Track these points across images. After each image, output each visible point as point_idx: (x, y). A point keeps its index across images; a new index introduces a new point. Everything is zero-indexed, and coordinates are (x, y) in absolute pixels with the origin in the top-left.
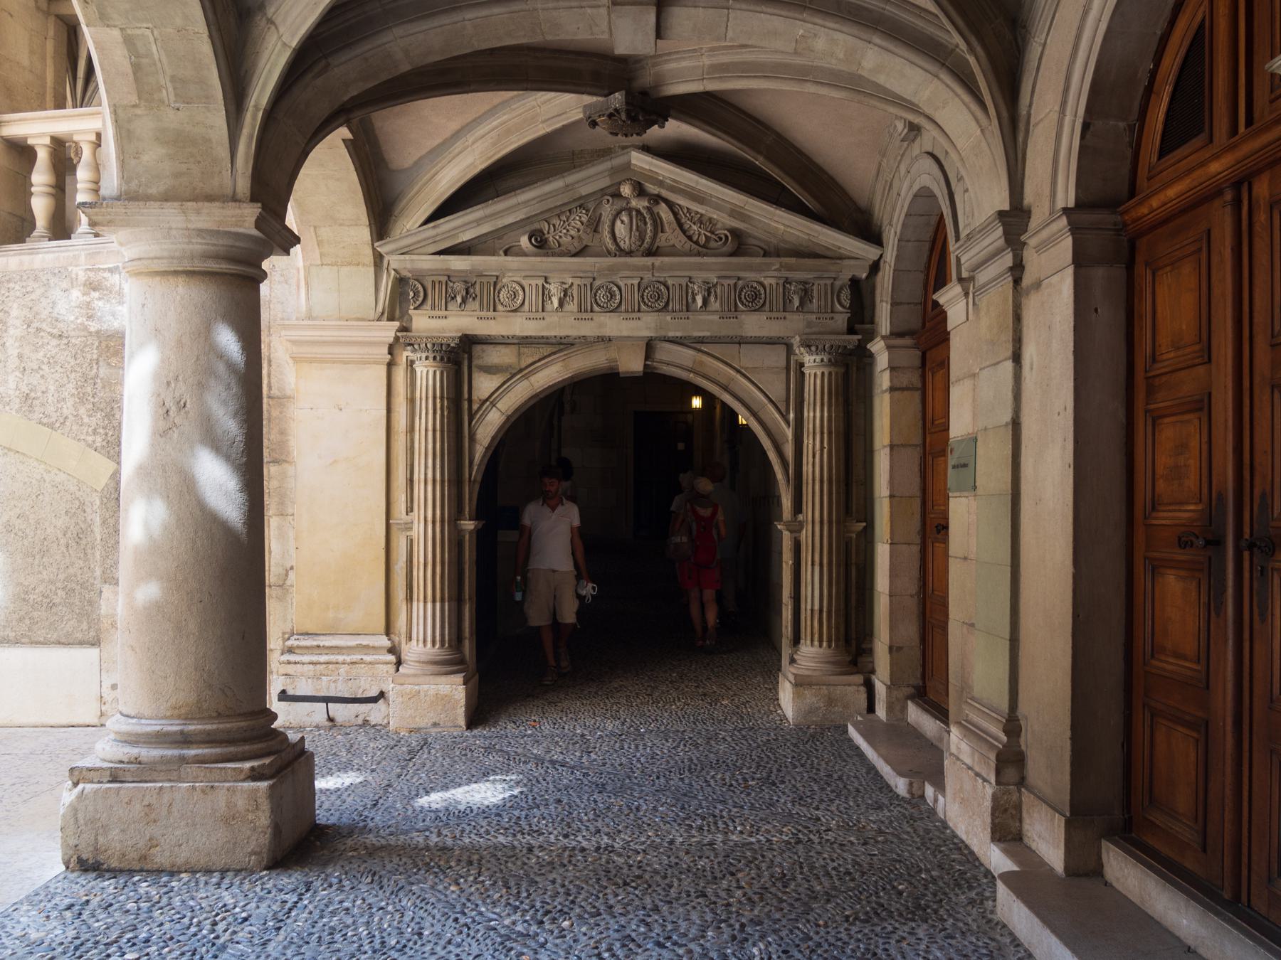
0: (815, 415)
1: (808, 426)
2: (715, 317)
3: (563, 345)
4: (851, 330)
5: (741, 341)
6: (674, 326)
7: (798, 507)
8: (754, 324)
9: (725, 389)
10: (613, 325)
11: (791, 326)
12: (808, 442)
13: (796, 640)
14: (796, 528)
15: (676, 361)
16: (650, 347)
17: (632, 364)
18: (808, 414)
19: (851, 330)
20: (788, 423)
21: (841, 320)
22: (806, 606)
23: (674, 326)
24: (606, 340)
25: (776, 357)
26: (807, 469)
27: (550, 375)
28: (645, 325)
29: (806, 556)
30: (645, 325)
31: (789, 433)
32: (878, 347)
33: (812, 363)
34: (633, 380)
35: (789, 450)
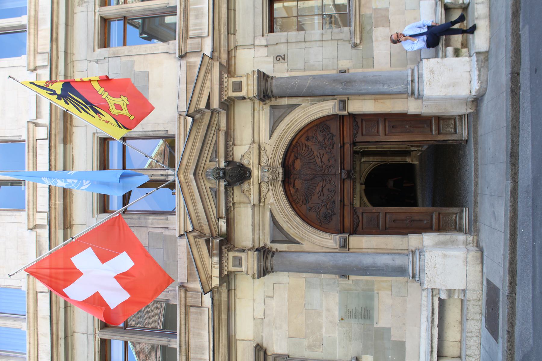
0: (371, 159)
1: (373, 160)
2: (357, 174)
3: (361, 197)
4: (358, 154)
5: (360, 170)
6: (358, 181)
7: (385, 161)
8: (358, 169)
9: (367, 172)
10: (358, 189)
11: (358, 163)
12: (375, 160)
13: (406, 161)
14: (389, 162)
15: (363, 180)
16: (361, 184)
17: (363, 187)
18: (371, 160)
19: (359, 154)
20: (372, 163)
21: (357, 155)
22: (401, 160)
23: (358, 181)
24: (360, 191)
25: (362, 165)
26: (380, 160)
27: (365, 199)
28: (358, 185)
29: (393, 160)
30: (358, 185)
31: (374, 163)
32: (361, 151)
33: (364, 159)
34: (365, 187)
35: (376, 163)
